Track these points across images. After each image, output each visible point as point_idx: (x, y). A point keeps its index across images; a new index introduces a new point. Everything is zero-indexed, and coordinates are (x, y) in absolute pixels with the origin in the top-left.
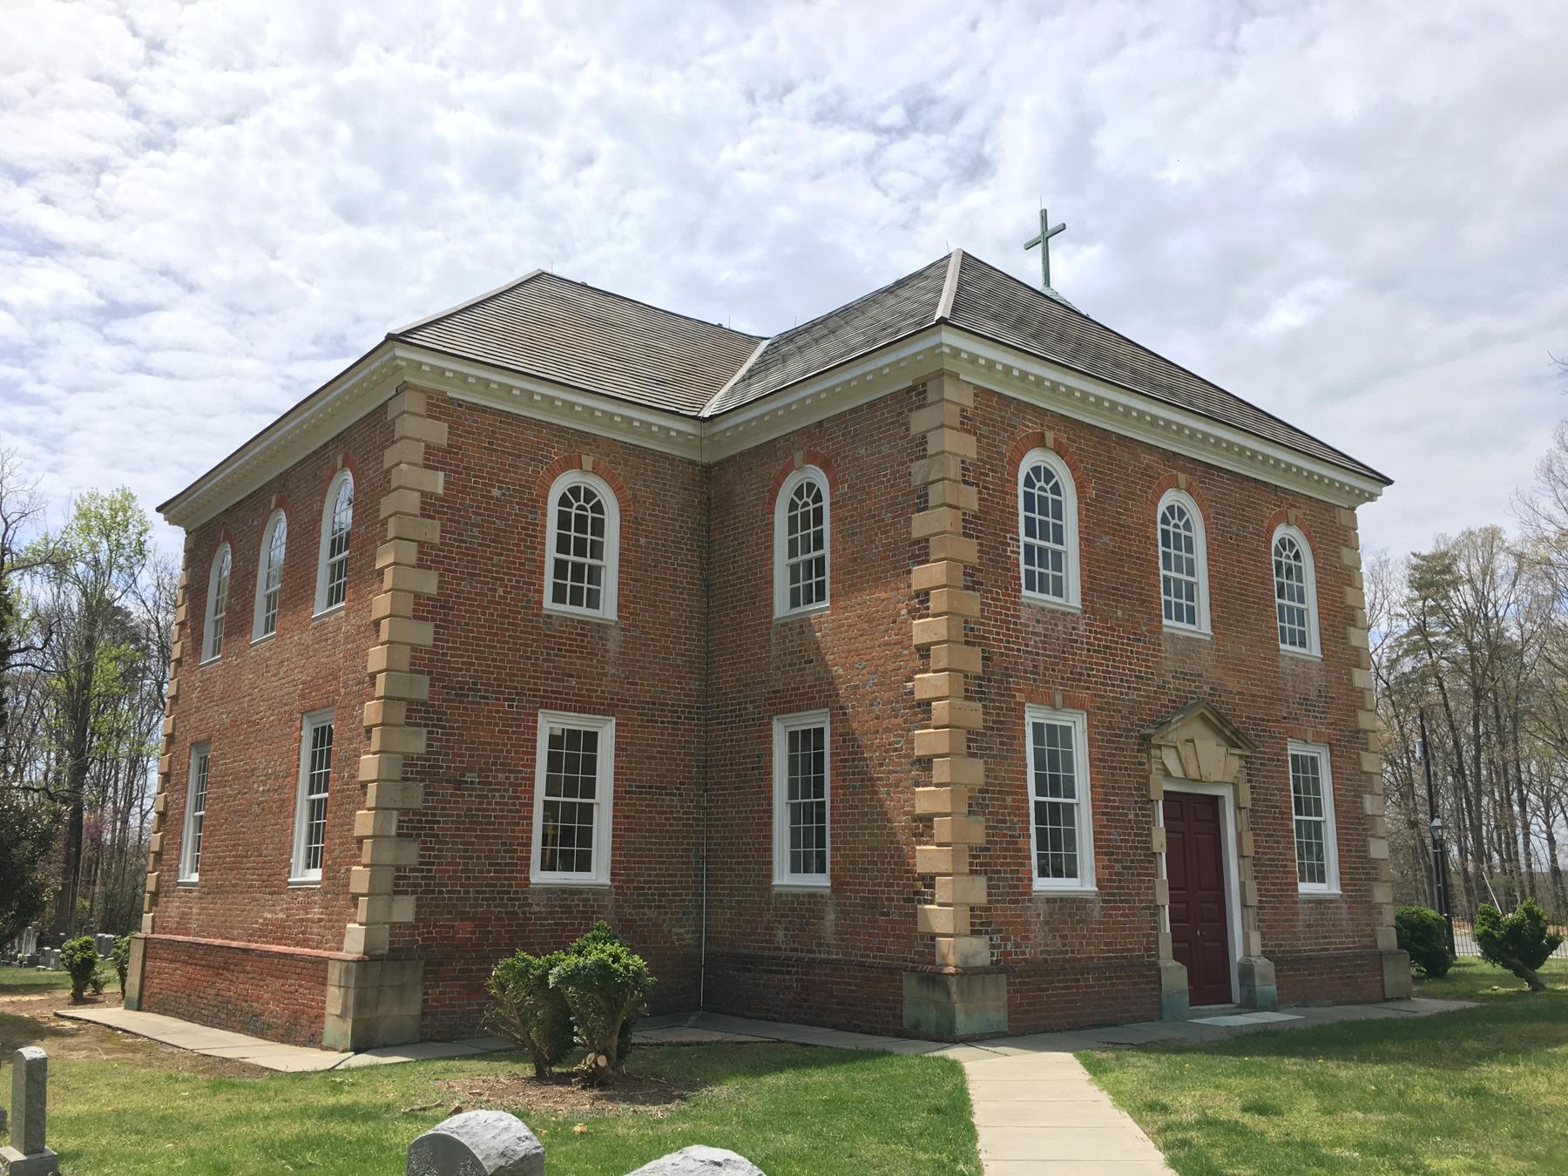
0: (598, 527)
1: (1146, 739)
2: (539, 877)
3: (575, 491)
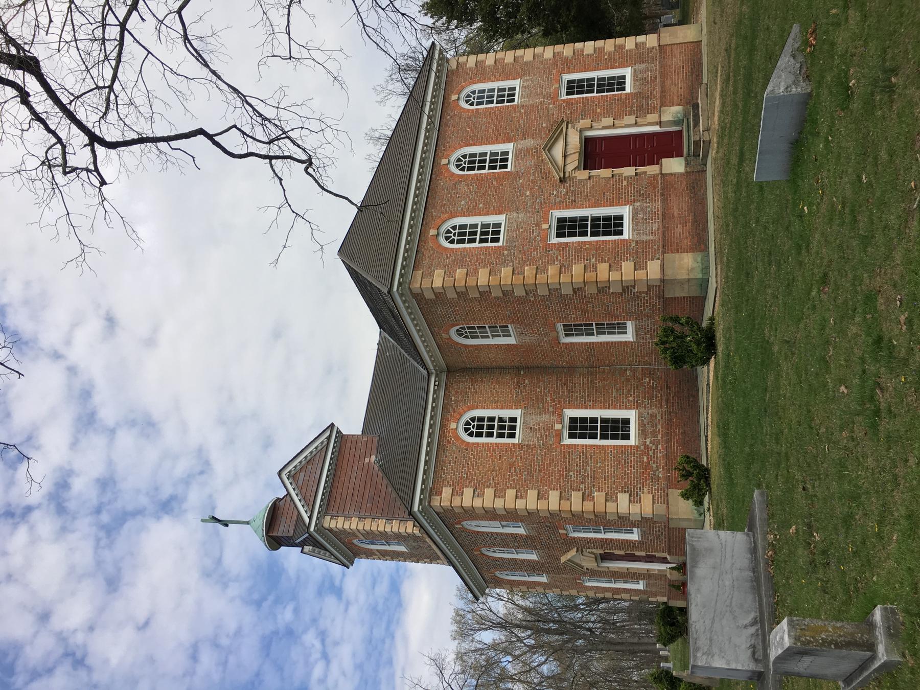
0: (481, 419)
1: (562, 180)
2: (632, 442)
3: (466, 430)
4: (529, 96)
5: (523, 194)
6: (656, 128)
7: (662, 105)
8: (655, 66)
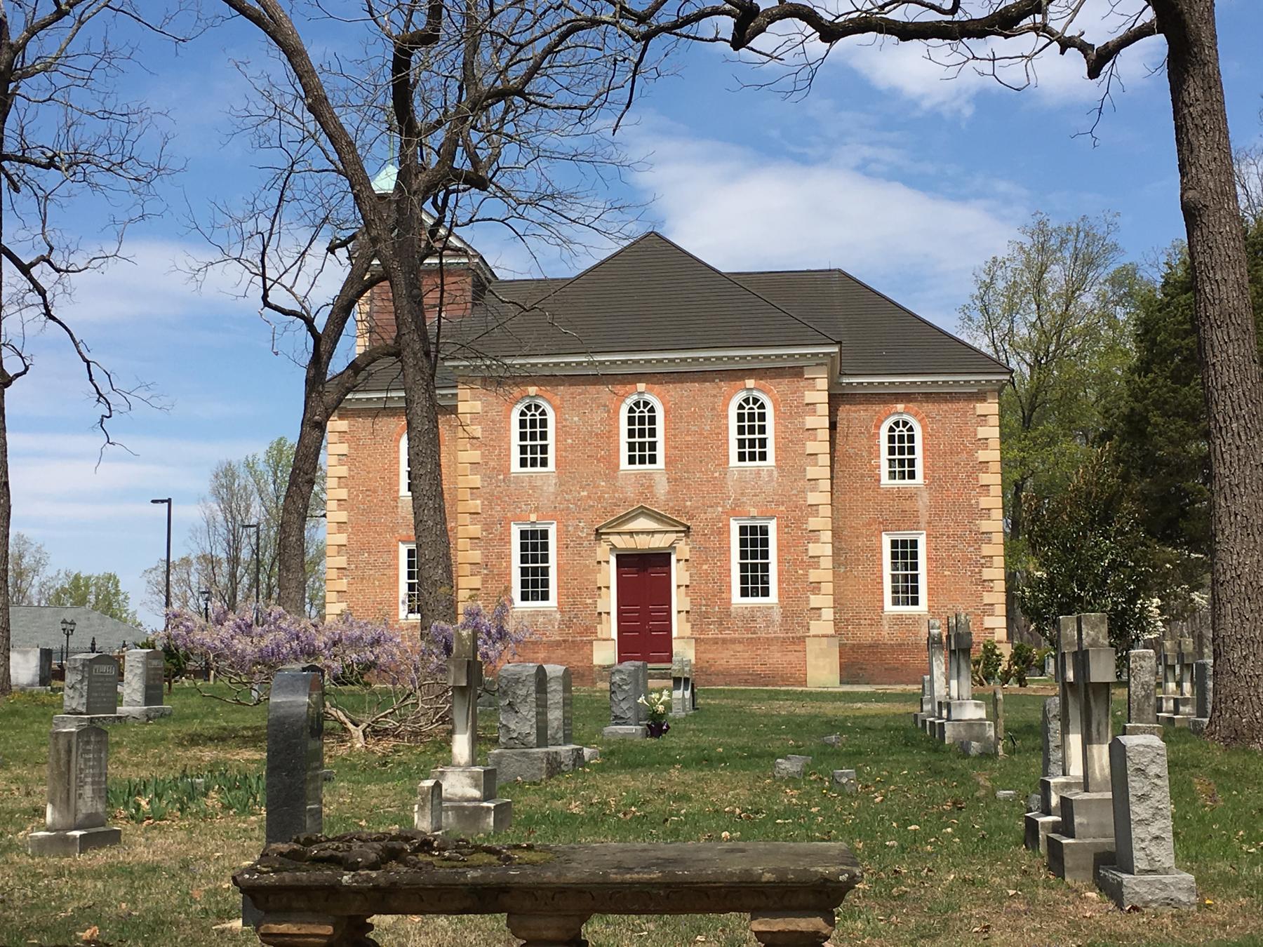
4: (740, 480)
5: (583, 488)
6: (675, 634)
7: (696, 640)
8: (776, 631)
